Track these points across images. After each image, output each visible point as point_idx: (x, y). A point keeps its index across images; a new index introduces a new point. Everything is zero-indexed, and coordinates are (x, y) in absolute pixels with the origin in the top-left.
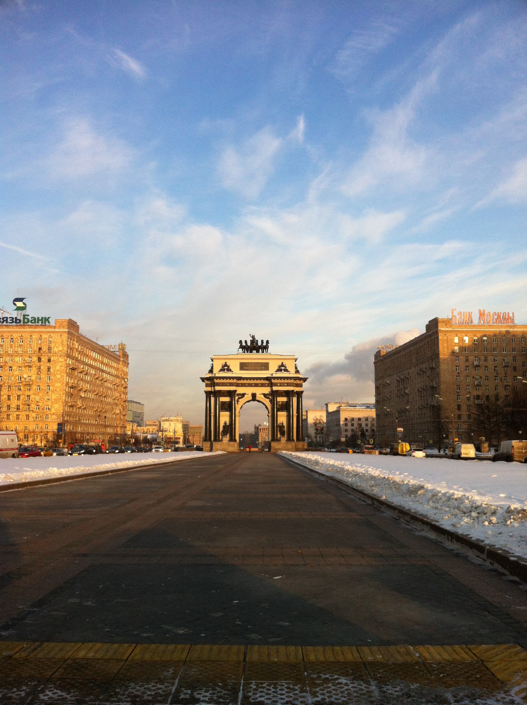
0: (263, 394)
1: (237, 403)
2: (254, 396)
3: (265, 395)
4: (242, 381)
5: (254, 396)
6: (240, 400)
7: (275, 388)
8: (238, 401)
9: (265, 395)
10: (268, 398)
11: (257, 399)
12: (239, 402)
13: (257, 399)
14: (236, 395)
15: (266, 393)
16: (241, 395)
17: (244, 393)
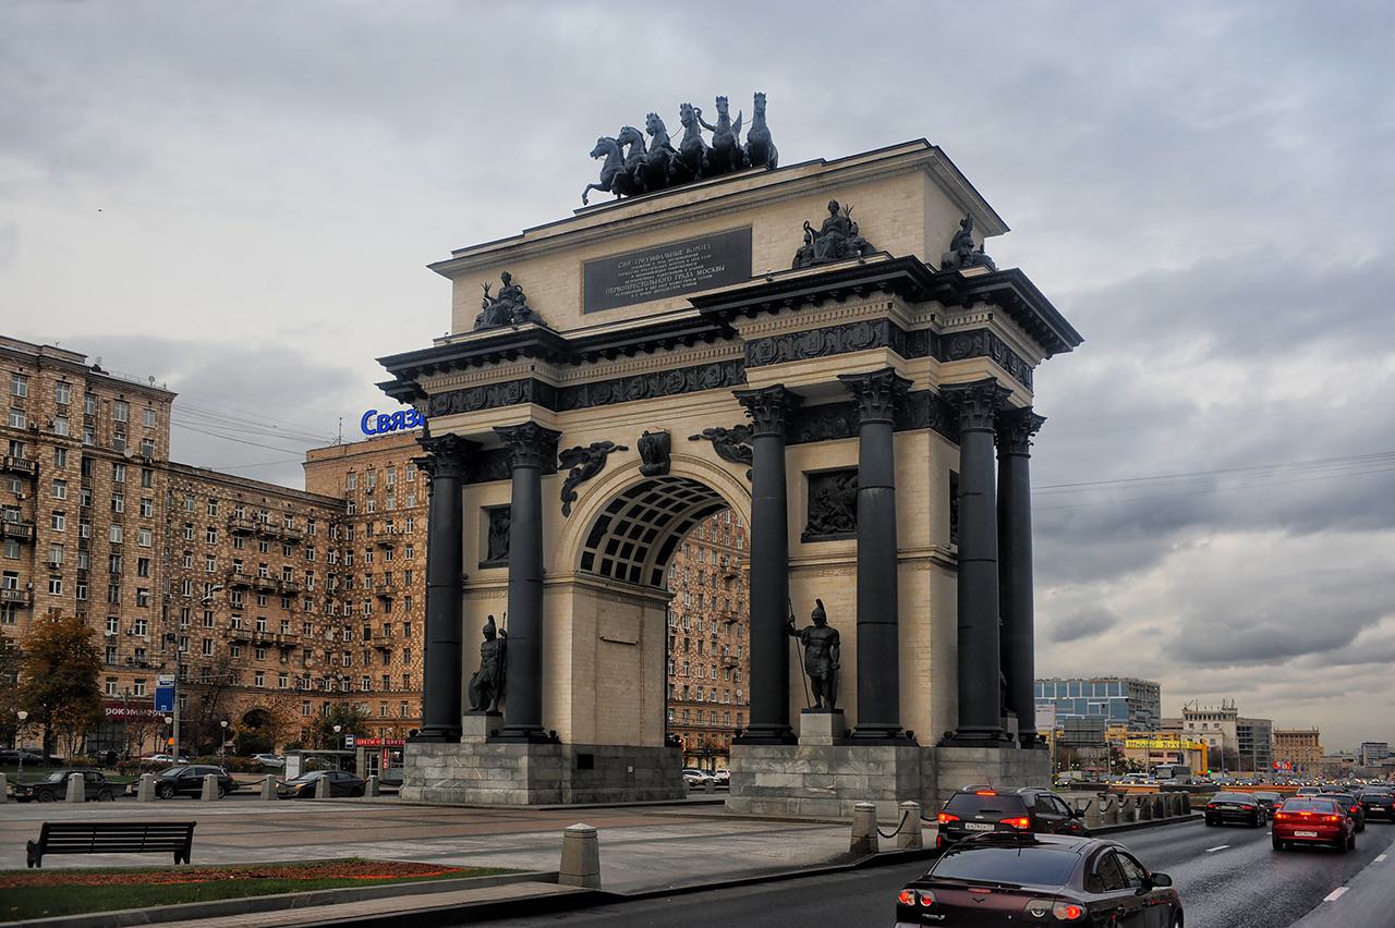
0: (710, 435)
1: (566, 511)
2: (656, 450)
3: (724, 441)
4: (584, 374)
5: (656, 450)
6: (581, 490)
7: (759, 378)
8: (568, 496)
9: (724, 441)
10: (743, 457)
11: (679, 468)
12: (573, 505)
13: (679, 468)
14: (559, 464)
15: (730, 427)
16: (584, 462)
17: (600, 438)
